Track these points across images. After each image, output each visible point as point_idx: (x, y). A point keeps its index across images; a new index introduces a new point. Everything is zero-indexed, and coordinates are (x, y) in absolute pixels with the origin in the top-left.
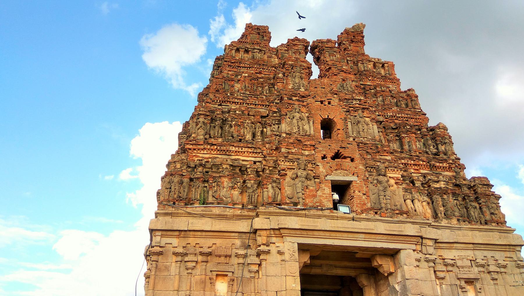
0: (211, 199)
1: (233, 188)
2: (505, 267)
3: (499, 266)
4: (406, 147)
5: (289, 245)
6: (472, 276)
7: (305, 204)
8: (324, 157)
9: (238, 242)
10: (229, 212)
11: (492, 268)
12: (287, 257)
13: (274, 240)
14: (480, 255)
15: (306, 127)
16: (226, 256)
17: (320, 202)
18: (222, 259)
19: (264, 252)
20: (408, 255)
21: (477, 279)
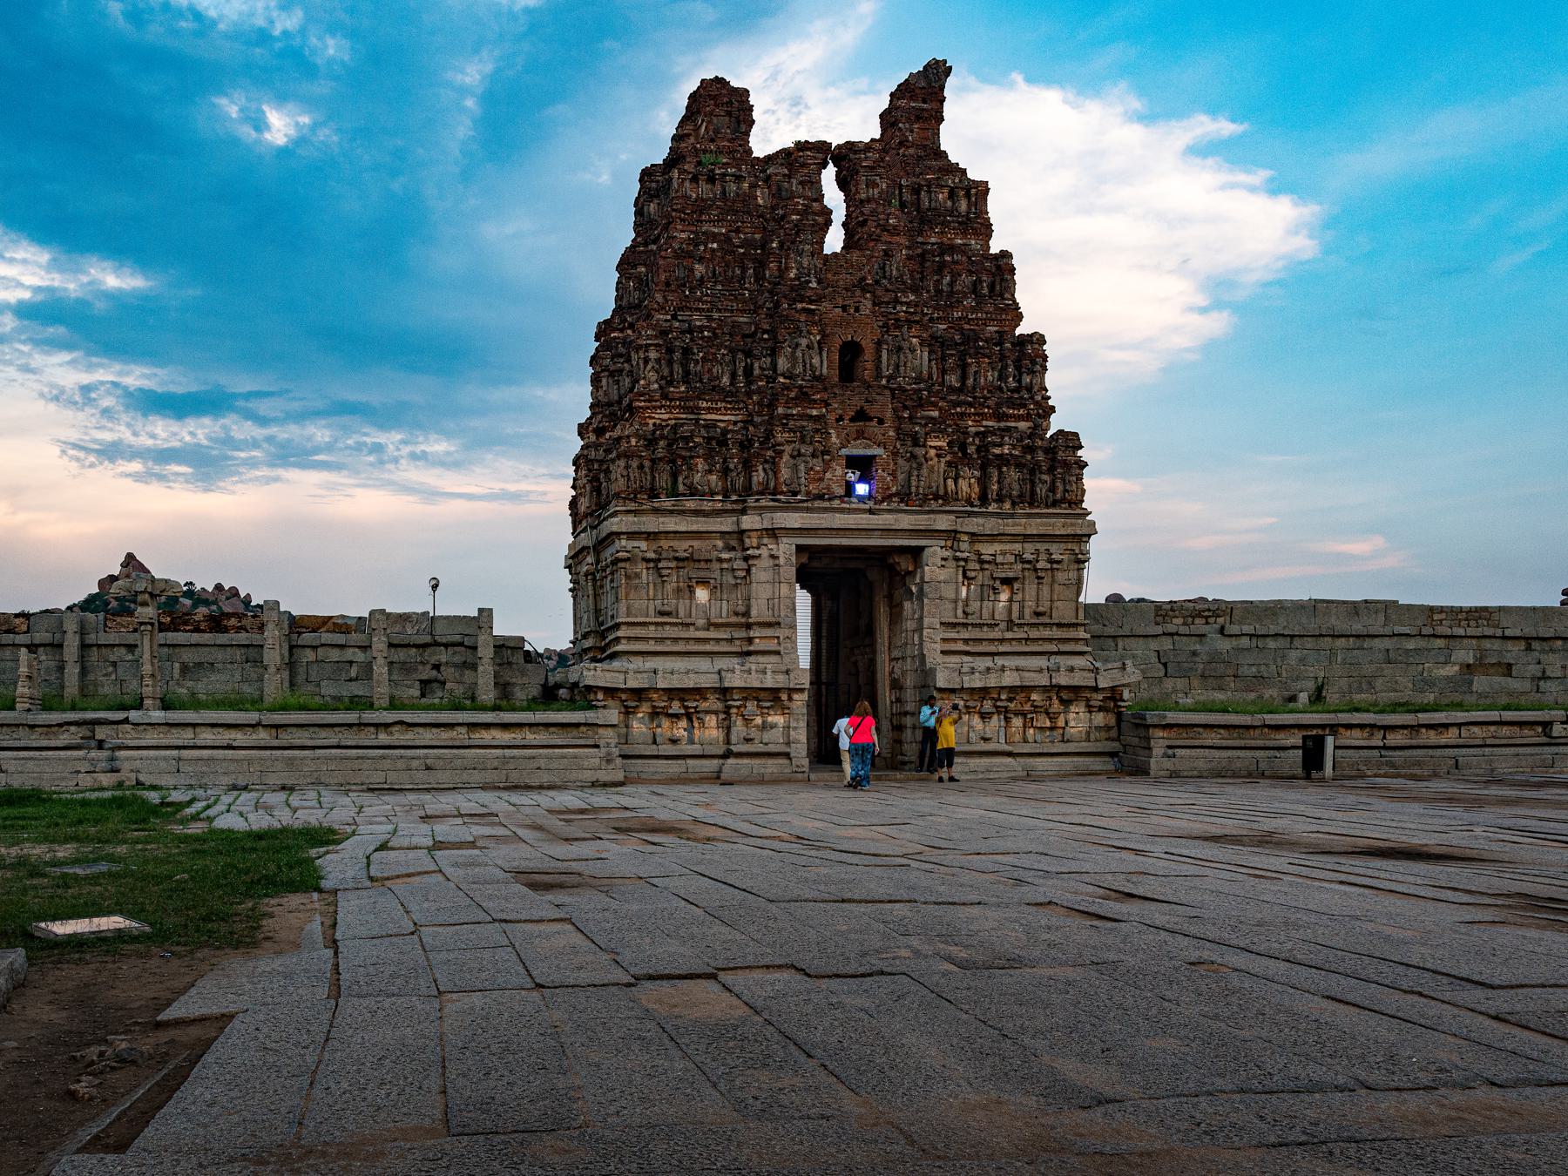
0: (681, 488)
1: (710, 472)
2: (1058, 562)
3: (1051, 561)
4: (970, 382)
5: (786, 549)
6: (1011, 575)
7: (808, 493)
8: (840, 419)
9: (720, 544)
10: (707, 506)
11: (1040, 565)
12: (782, 561)
13: (765, 541)
14: (1029, 550)
15: (816, 361)
16: (707, 561)
17: (828, 488)
18: (703, 565)
19: (754, 557)
20: (935, 552)
21: (1016, 579)
